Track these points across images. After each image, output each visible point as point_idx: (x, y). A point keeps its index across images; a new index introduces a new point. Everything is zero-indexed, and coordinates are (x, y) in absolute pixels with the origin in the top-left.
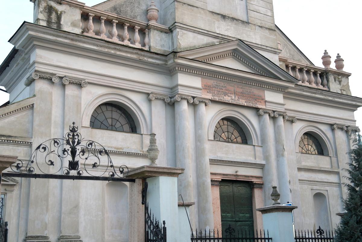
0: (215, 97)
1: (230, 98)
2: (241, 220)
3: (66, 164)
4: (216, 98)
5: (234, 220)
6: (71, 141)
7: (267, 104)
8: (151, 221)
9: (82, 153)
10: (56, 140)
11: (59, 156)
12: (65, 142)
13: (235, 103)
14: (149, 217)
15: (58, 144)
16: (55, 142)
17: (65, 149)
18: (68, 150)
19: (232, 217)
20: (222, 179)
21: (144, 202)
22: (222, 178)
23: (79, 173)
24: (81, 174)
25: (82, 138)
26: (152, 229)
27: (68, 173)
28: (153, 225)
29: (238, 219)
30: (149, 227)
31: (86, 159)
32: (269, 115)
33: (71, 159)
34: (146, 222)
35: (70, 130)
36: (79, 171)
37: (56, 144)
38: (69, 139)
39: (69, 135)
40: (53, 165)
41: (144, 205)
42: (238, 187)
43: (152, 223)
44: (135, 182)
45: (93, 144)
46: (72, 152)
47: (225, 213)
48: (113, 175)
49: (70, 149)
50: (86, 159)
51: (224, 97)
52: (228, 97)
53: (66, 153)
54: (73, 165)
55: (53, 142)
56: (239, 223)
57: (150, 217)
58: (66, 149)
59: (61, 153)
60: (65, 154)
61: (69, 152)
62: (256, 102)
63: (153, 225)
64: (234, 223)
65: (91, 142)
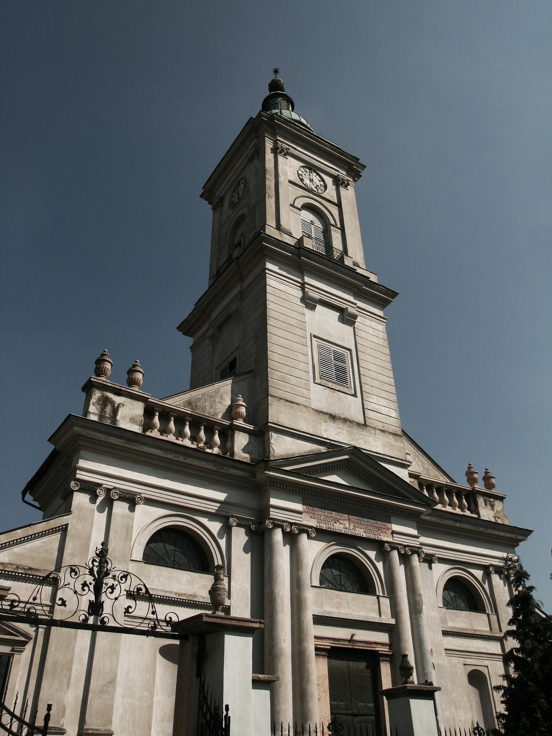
2: (361, 712)
3: (85, 606)
5: (350, 712)
6: (96, 569)
8: (207, 705)
9: (110, 590)
10: (74, 568)
11: (76, 592)
12: (87, 571)
14: (205, 699)
15: (76, 574)
16: (72, 570)
17: (85, 582)
18: (90, 584)
21: (199, 674)
23: (102, 621)
24: (106, 622)
25: (113, 567)
26: (208, 718)
27: (86, 619)
28: (211, 713)
29: (355, 711)
30: (205, 716)
31: (116, 599)
33: (93, 598)
34: (200, 707)
35: (96, 554)
36: (104, 617)
37: (73, 574)
38: (93, 567)
39: (94, 560)
40: (65, 606)
41: (199, 679)
43: (209, 708)
44: (187, 640)
45: (129, 577)
46: (95, 587)
48: (155, 627)
49: (93, 583)
50: (116, 599)
53: (86, 588)
54: (96, 607)
55: (69, 570)
56: (358, 718)
57: (207, 699)
58: (88, 583)
59: (79, 589)
60: (84, 590)
61: (92, 587)
63: (211, 713)
64: (350, 717)
65: (125, 573)
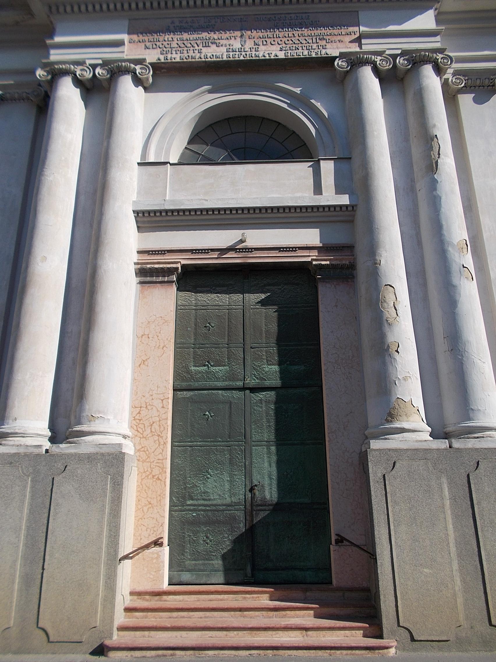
0: (169, 56)
1: (223, 49)
4: (174, 55)
5: (240, 384)
7: (364, 41)
13: (242, 58)
19: (232, 377)
20: (183, 266)
22: (184, 262)
29: (252, 382)
32: (376, 71)
42: (265, 285)
47: (205, 365)
51: (204, 50)
52: (216, 48)
62: (323, 43)
64: (236, 394)
